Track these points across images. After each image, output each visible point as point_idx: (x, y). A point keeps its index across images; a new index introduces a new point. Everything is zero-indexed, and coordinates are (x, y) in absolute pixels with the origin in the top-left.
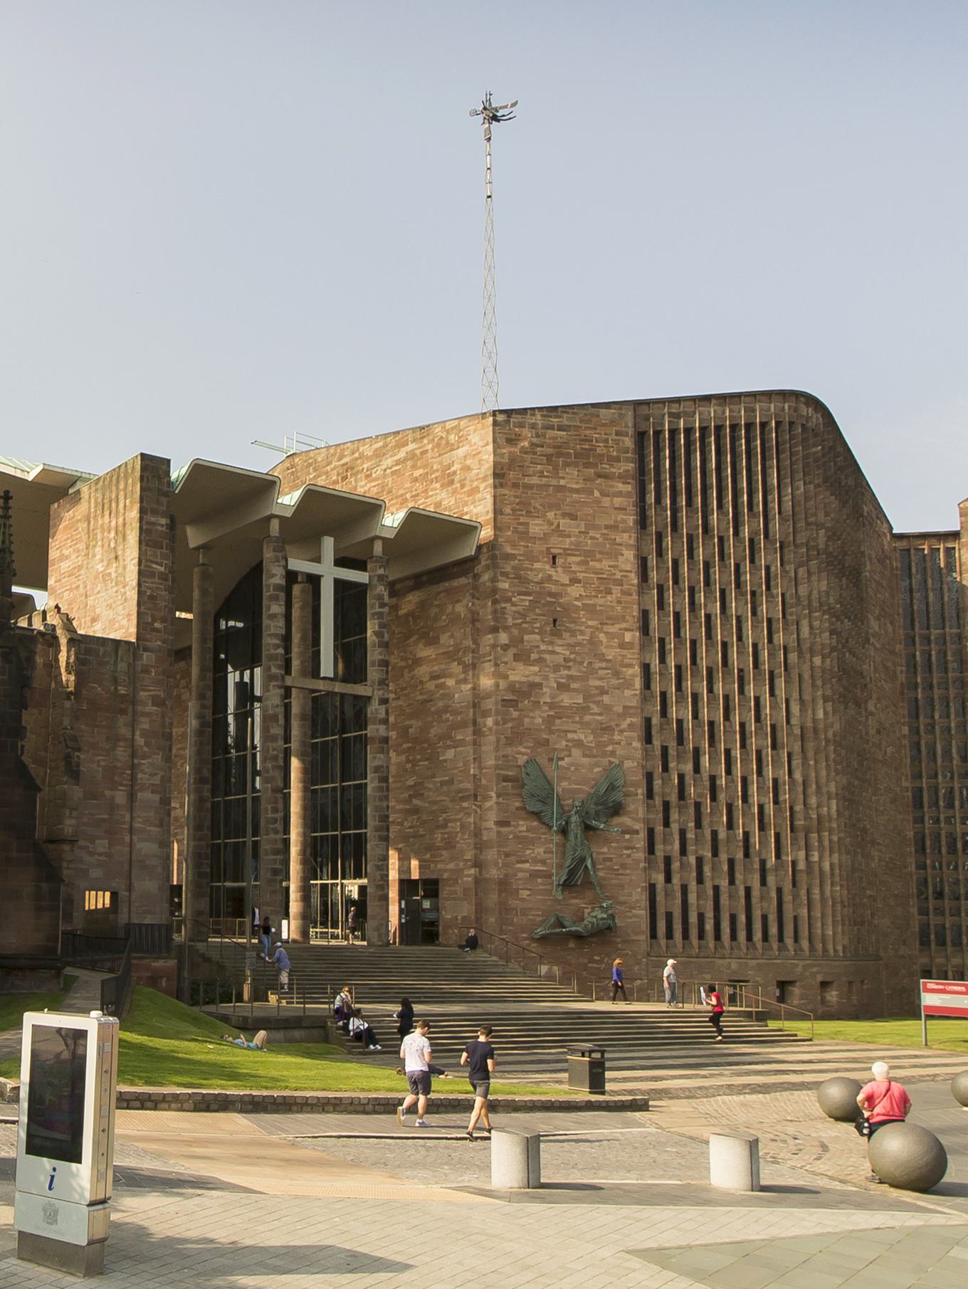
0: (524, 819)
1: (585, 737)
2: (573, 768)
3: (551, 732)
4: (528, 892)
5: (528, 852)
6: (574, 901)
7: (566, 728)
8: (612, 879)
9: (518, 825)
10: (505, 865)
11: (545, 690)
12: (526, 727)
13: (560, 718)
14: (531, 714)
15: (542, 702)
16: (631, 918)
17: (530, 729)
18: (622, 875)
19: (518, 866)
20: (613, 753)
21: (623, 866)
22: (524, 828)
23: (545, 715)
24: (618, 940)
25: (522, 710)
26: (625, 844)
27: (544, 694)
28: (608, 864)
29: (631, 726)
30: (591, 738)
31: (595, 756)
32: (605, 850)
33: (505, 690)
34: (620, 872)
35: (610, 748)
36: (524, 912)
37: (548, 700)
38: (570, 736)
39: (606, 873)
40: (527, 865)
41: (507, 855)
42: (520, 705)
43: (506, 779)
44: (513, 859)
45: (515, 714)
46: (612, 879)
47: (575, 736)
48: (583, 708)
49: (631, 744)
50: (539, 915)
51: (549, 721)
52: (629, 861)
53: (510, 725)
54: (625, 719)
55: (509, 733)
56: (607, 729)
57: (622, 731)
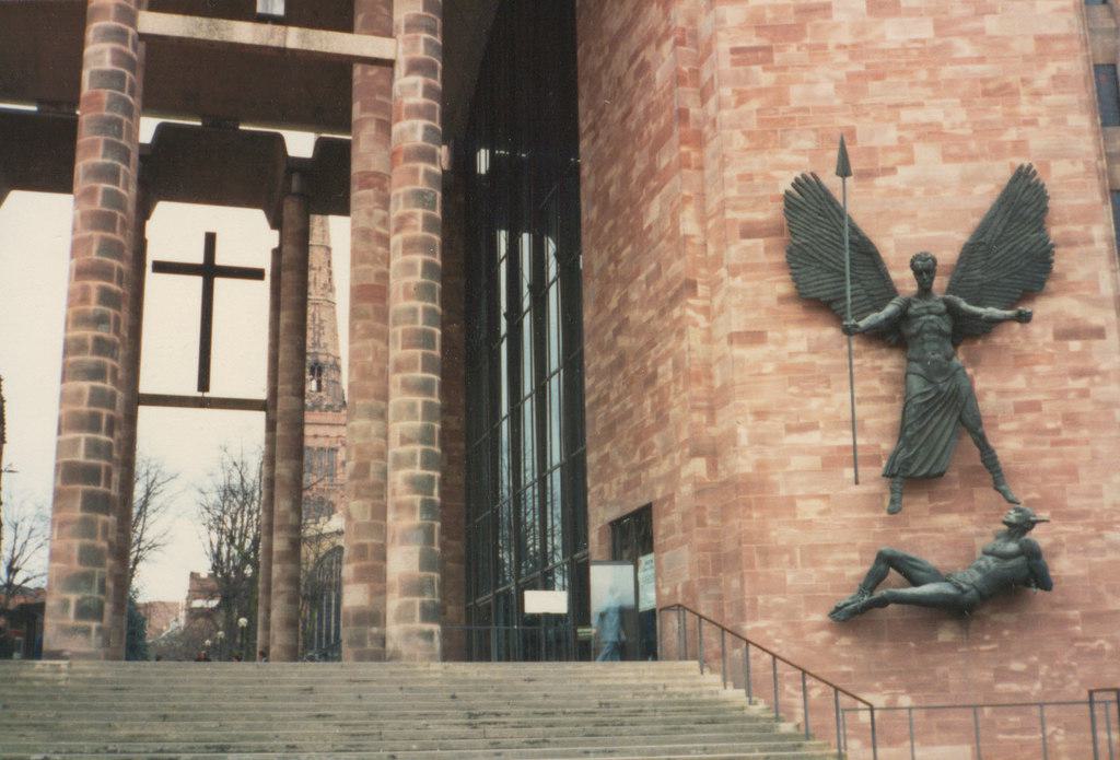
0: (801, 322)
1: (947, 115)
2: (919, 192)
3: (859, 111)
4: (819, 504)
5: (815, 403)
6: (946, 520)
7: (898, 99)
8: (1043, 455)
9: (786, 340)
10: (759, 440)
11: (838, 16)
12: (794, 103)
13: (879, 77)
14: (806, 75)
15: (832, 43)
16: (1102, 552)
17: (805, 110)
18: (1068, 442)
19: (795, 439)
20: (1019, 146)
21: (1071, 420)
22: (802, 346)
23: (841, 74)
24: (1074, 613)
25: (784, 68)
26: (1071, 364)
27: (836, 26)
28: (1030, 417)
29: (1059, 81)
30: (961, 115)
31: (972, 157)
32: (1019, 381)
33: (741, 27)
34: (1065, 435)
35: (1011, 135)
36: (813, 555)
37: (847, 39)
38: (907, 116)
39: (1027, 443)
40: (813, 438)
41: (760, 414)
42: (777, 58)
43: (749, 231)
44: (776, 423)
45: (766, 78)
46: (1043, 455)
47: (921, 116)
48: (936, 50)
49: (1063, 121)
50: (851, 562)
51: (853, 85)
52: (1085, 407)
53: (754, 104)
54: (1042, 66)
55: (753, 124)
56: (1002, 92)
57: (1037, 94)
